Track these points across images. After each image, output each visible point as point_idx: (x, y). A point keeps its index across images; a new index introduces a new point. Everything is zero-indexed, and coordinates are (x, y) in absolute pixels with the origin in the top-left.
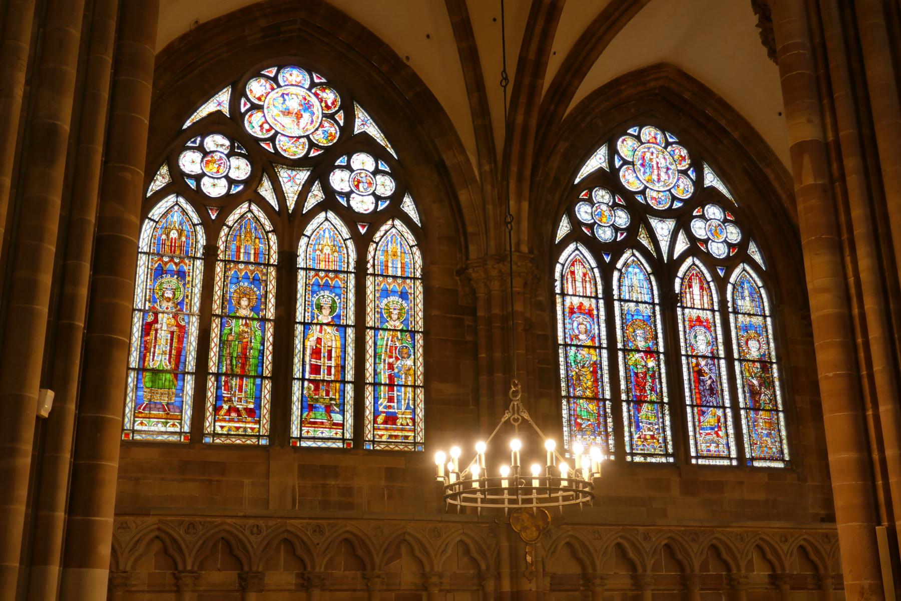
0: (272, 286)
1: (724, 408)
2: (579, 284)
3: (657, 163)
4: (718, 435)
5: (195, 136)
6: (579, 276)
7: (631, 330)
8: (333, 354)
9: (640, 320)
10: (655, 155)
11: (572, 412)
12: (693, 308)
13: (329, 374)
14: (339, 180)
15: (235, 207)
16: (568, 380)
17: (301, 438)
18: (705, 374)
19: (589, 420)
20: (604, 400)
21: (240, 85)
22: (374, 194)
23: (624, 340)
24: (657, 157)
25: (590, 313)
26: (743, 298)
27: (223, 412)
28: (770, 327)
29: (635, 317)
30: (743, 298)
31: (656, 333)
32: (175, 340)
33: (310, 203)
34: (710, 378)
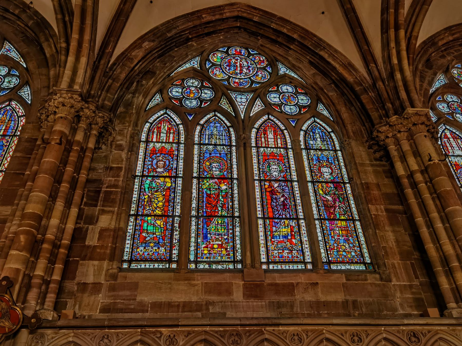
1: (298, 219)
3: (240, 64)
4: (291, 243)
7: (208, 164)
9: (217, 157)
10: (239, 61)
12: (268, 147)
16: (139, 202)
18: (278, 194)
19: (153, 234)
23: (199, 171)
24: (240, 61)
26: (315, 139)
28: (341, 158)
29: (212, 155)
30: (315, 139)
31: (232, 165)
34: (283, 196)
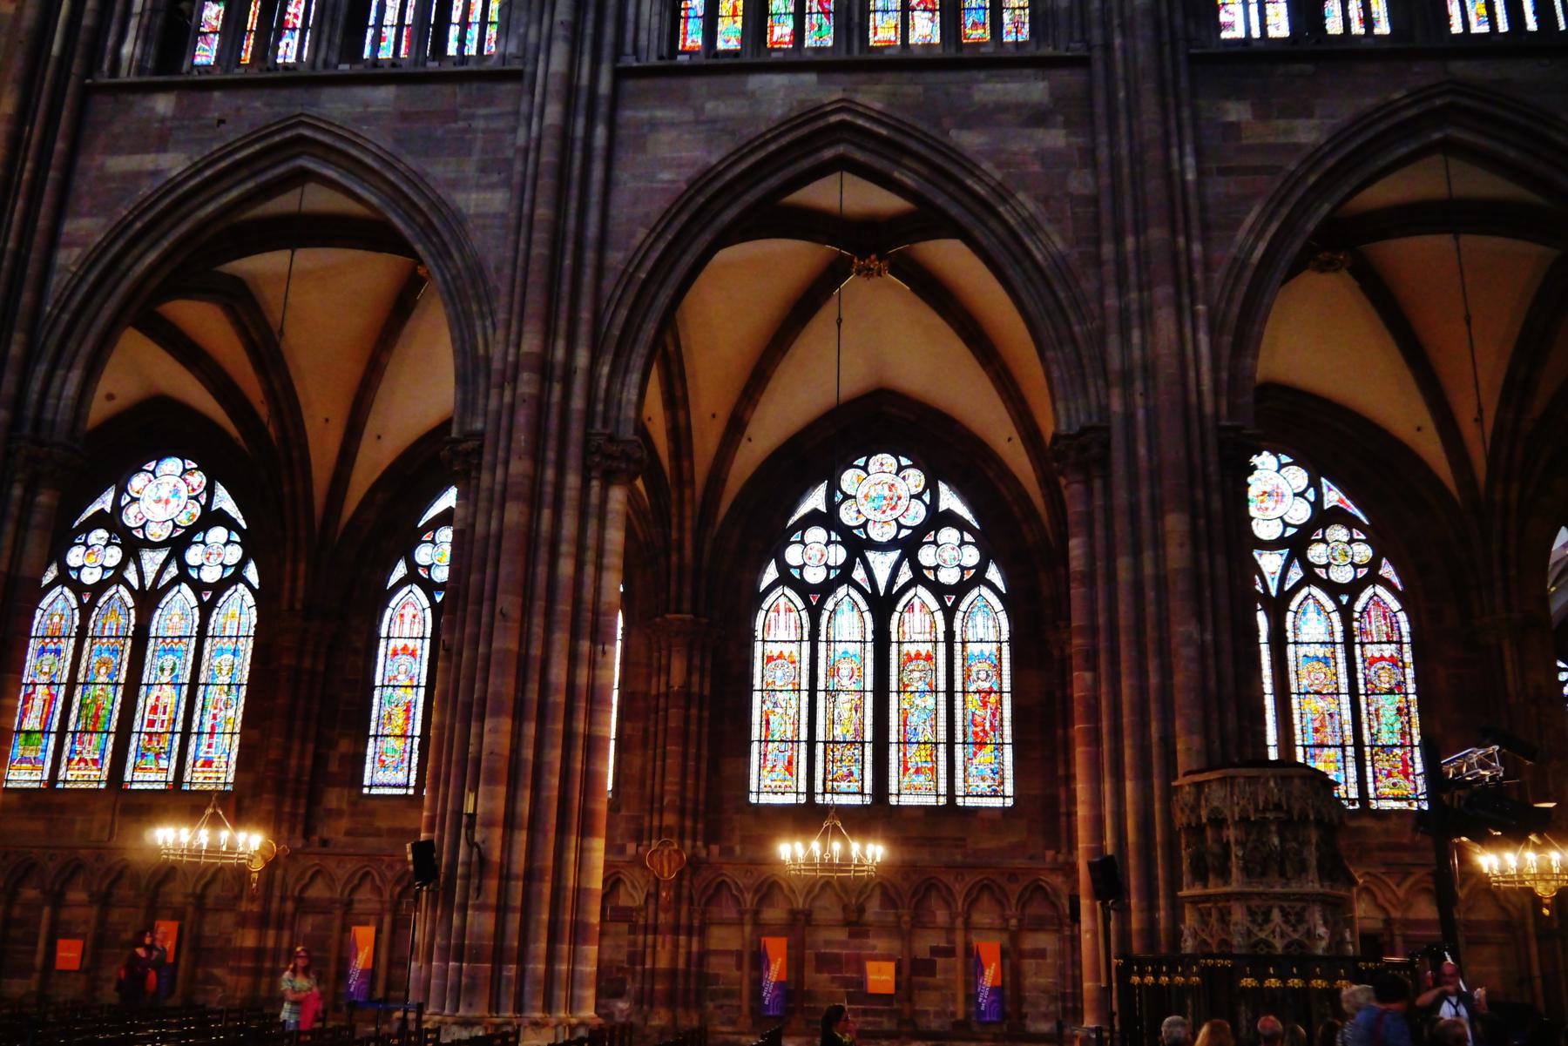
0: (126, 655)
2: (407, 626)
5: (81, 533)
6: (408, 619)
8: (168, 709)
11: (378, 750)
13: (162, 726)
14: (193, 556)
15: (105, 591)
17: (132, 782)
20: (413, 737)
21: (121, 483)
22: (222, 564)
25: (413, 654)
27: (74, 763)
32: (47, 706)
33: (167, 578)
